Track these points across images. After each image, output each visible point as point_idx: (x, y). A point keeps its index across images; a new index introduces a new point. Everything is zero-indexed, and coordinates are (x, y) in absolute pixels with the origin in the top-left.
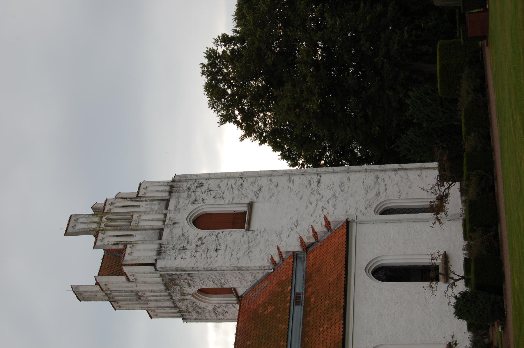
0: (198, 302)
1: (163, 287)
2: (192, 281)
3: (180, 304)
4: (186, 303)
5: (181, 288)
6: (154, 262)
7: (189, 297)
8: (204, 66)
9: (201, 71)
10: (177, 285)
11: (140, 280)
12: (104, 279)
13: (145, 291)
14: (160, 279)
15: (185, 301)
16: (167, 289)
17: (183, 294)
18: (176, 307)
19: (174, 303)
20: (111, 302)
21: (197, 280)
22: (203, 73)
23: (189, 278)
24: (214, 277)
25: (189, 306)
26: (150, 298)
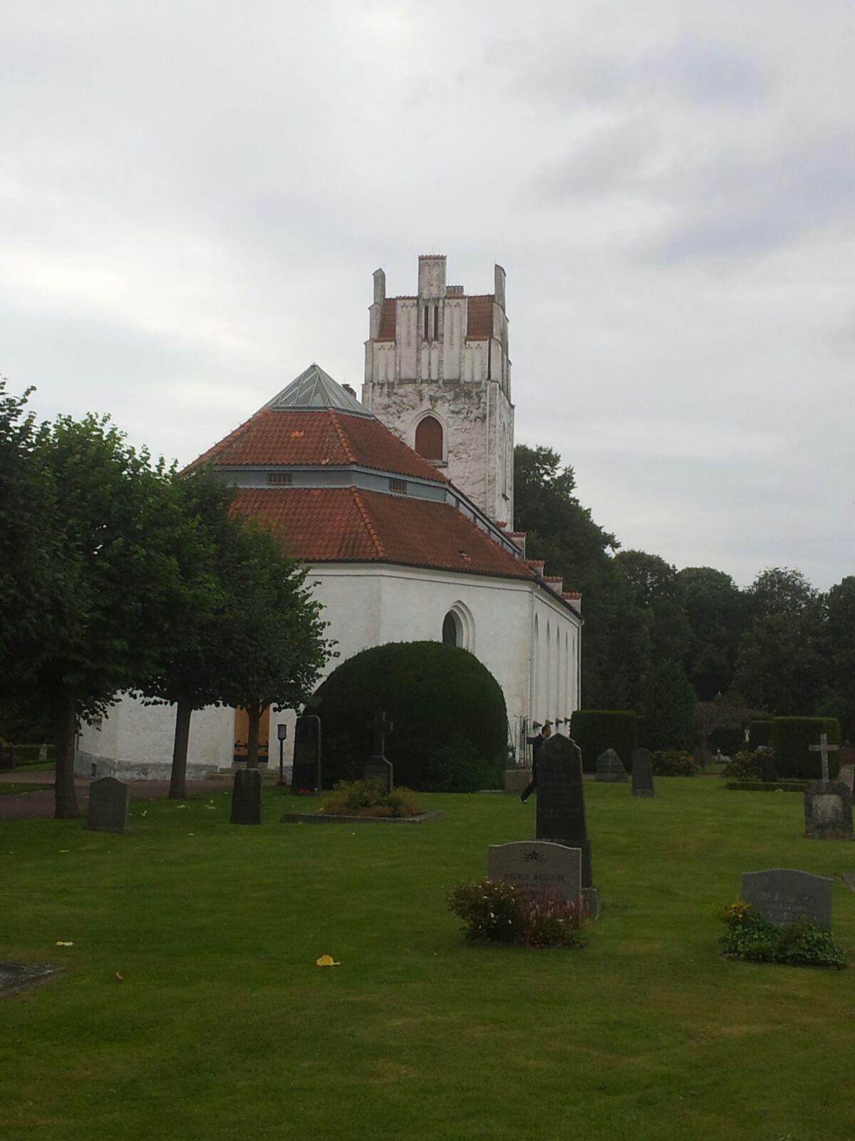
0: (415, 413)
1: (446, 376)
2: (466, 418)
3: (410, 388)
4: (414, 398)
5: (449, 401)
6: (492, 378)
7: (426, 405)
8: (551, 451)
9: (544, 447)
10: (456, 397)
11: (468, 353)
12: (464, 304)
13: (441, 351)
14: (467, 377)
15: (418, 398)
16: (446, 383)
17: (433, 400)
18: (402, 382)
19: (413, 381)
20: (417, 298)
21: (467, 425)
22: (541, 449)
23: (472, 416)
24: (472, 447)
25: (404, 399)
26: (424, 354)
